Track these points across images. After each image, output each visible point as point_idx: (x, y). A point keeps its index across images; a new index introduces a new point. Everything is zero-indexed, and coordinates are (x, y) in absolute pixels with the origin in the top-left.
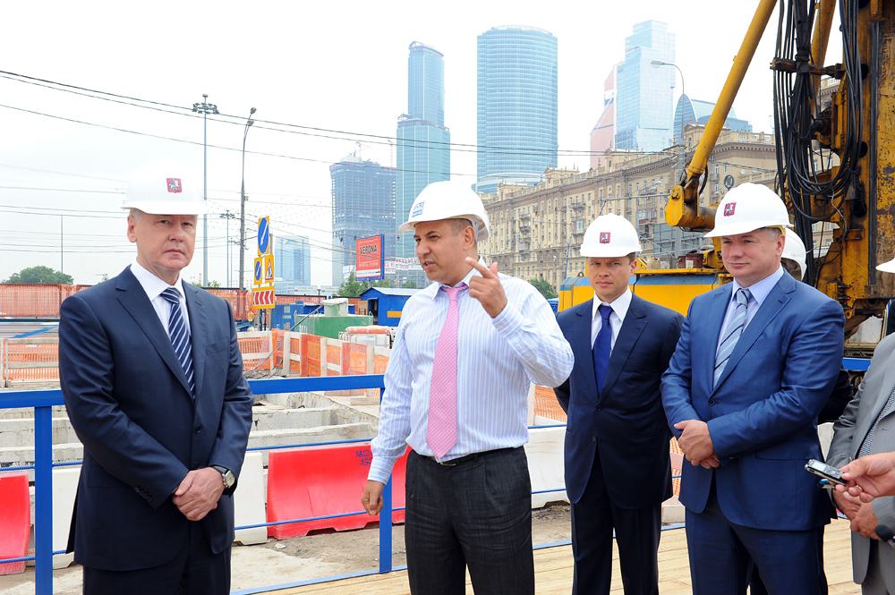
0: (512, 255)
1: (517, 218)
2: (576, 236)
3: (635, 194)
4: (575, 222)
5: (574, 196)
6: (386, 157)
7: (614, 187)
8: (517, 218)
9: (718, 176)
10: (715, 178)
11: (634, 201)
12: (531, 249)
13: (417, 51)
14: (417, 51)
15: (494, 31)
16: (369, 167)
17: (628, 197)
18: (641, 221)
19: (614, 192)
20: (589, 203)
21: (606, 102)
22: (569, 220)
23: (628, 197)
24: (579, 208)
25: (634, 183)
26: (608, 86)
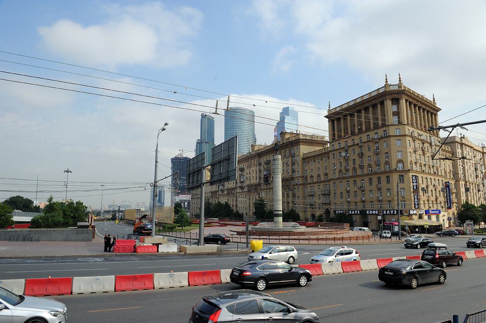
2: (241, 182)
3: (263, 164)
4: (240, 176)
9: (294, 154)
10: (293, 155)
11: (262, 166)
17: (260, 164)
18: (264, 175)
19: (254, 163)
20: (246, 168)
23: (260, 164)
25: (262, 158)
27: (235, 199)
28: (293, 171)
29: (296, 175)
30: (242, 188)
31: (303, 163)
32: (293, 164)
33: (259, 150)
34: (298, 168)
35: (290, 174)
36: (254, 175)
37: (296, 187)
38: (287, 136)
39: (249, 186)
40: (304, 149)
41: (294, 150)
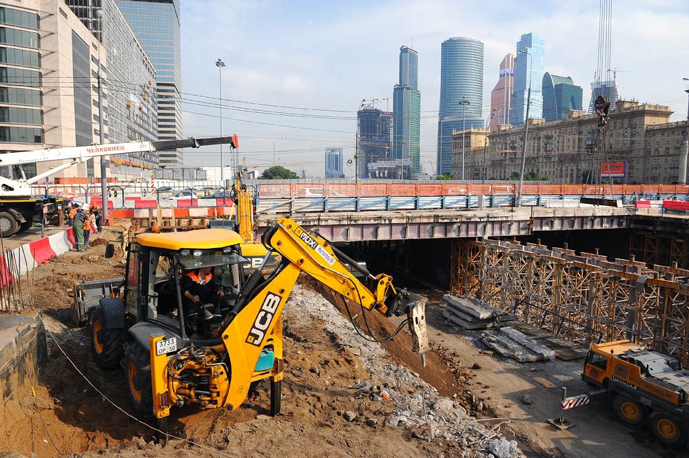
0: (505, 160)
1: (509, 142)
5: (545, 133)
6: (386, 106)
7: (572, 129)
8: (509, 142)
12: (517, 157)
13: (404, 50)
14: (404, 50)
15: (451, 41)
16: (377, 112)
17: (580, 133)
20: (555, 136)
21: (501, 76)
22: (542, 145)
24: (549, 138)
26: (502, 66)
27: (503, 171)
28: (632, 142)
29: (636, 146)
30: (548, 157)
31: (646, 136)
32: (632, 135)
33: (579, 117)
34: (640, 139)
35: (628, 145)
36: (571, 144)
37: (635, 159)
38: (627, 106)
39: (560, 156)
40: (648, 121)
41: (636, 121)
